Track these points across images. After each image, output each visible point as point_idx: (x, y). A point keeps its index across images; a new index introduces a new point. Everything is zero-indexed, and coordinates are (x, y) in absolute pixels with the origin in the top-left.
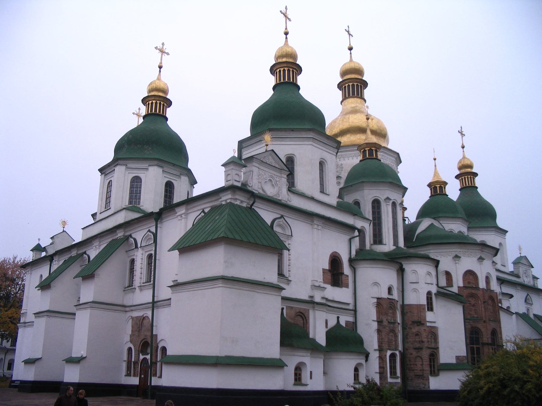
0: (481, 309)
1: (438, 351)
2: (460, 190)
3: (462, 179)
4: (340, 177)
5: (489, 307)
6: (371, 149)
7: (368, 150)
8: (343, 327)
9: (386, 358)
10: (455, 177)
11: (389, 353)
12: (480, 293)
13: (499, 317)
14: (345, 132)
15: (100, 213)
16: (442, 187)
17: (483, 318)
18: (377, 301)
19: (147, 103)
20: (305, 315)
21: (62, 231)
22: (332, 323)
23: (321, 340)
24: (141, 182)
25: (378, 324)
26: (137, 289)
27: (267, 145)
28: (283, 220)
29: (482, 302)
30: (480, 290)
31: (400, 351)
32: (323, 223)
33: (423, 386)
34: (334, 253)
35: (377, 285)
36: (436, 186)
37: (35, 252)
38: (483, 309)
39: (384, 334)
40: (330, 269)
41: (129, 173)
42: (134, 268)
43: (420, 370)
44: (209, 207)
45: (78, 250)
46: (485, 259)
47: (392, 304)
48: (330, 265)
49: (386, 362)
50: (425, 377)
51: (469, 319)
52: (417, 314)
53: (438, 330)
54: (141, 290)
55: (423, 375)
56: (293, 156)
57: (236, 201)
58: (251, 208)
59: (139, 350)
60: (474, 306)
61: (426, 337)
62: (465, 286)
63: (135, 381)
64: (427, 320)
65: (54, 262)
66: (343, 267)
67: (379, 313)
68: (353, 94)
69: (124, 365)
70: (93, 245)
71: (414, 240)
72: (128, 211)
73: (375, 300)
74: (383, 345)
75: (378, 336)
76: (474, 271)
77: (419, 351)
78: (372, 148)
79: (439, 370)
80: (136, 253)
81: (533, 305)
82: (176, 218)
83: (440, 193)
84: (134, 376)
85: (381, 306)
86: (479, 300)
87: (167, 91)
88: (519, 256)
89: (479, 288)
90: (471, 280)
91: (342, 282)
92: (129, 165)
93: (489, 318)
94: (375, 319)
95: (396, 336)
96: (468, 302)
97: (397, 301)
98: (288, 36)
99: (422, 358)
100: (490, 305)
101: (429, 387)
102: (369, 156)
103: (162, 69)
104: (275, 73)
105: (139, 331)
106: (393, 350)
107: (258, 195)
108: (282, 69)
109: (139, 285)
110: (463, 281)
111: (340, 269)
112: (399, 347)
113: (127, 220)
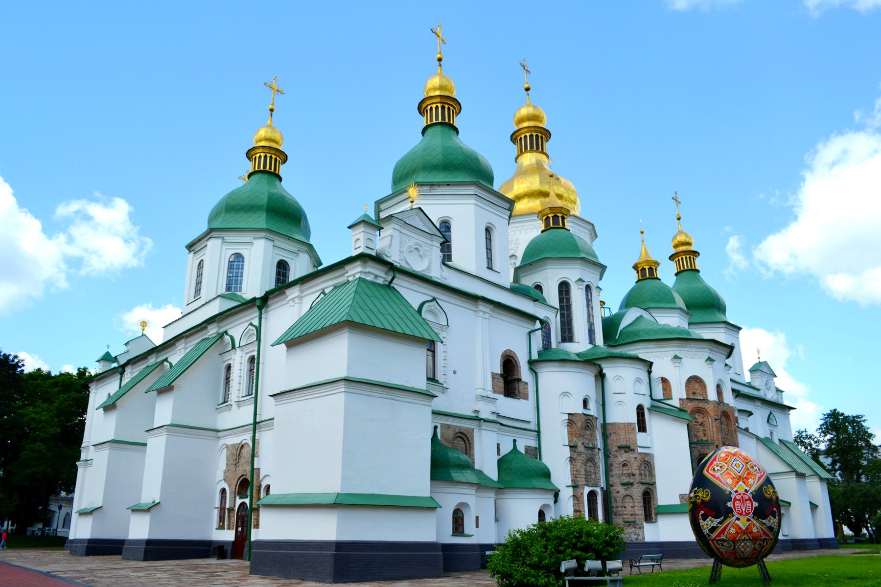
0: (713, 429)
1: (655, 487)
2: (676, 275)
3: (679, 260)
4: (514, 255)
5: (723, 427)
6: (556, 215)
7: (553, 217)
8: (522, 454)
9: (583, 498)
10: (668, 257)
11: (587, 490)
12: (710, 408)
13: (737, 440)
14: (521, 197)
15: (187, 305)
16: (653, 269)
17: (715, 442)
18: (569, 417)
19: (254, 157)
20: (468, 436)
21: (141, 335)
22: (506, 449)
23: (492, 472)
24: (243, 261)
25: (570, 450)
26: (234, 405)
27: (412, 202)
28: (435, 305)
29: (714, 420)
32: (491, 310)
33: (636, 536)
34: (507, 352)
35: (569, 397)
36: (645, 267)
37: (102, 364)
38: (714, 429)
39: (580, 464)
40: (502, 373)
41: (226, 249)
42: (230, 378)
43: (631, 515)
44: (332, 286)
45: (157, 357)
46: (714, 361)
47: (589, 421)
48: (502, 368)
49: (583, 503)
51: (696, 444)
52: (625, 437)
53: (653, 459)
54: (239, 407)
55: (635, 522)
56: (447, 220)
57: (368, 276)
58: (389, 286)
59: (235, 491)
60: (701, 424)
62: (689, 397)
63: (228, 536)
64: (639, 444)
65: (126, 375)
66: (520, 371)
67: (570, 434)
68: (532, 147)
69: (216, 514)
70: (177, 348)
71: (617, 337)
72: (222, 299)
73: (566, 417)
74: (578, 479)
75: (572, 466)
76: (700, 378)
77: (628, 488)
78: (557, 214)
79: (656, 514)
80: (233, 355)
81: (778, 427)
82: (286, 304)
83: (650, 277)
84: (229, 528)
85: (574, 425)
86: (709, 416)
87: (281, 142)
88: (758, 362)
90: (697, 389)
91: (519, 392)
92: (227, 239)
93: (723, 441)
94: (567, 444)
95: (595, 465)
96: (695, 420)
97: (597, 418)
98: (442, 63)
99: (633, 499)
102: (553, 225)
103: (273, 113)
104: (425, 111)
105: (236, 464)
106: (592, 486)
107: (401, 268)
108: (434, 106)
109: (237, 400)
110: (687, 391)
111: (516, 374)
112: (600, 482)
113: (221, 311)
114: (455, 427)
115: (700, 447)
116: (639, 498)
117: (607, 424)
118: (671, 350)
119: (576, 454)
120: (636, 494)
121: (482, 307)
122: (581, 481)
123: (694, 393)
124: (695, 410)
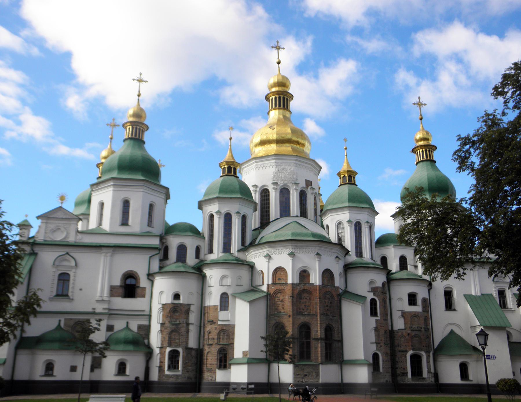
11: (168, 350)
18: (162, 306)
29: (289, 297)
30: (288, 285)
31: (188, 349)
43: (211, 364)
50: (213, 371)
61: (216, 334)
66: (139, 281)
73: (161, 306)
79: (230, 365)
89: (287, 283)
90: (282, 276)
100: (306, 299)
101: (215, 380)
106: (175, 347)
114: (75, 319)
115: (277, 317)
116: (215, 353)
117: (205, 307)
118: (265, 251)
119: (163, 328)
120: (214, 351)
121: (104, 250)
122: (166, 344)
123: (279, 279)
124: (277, 292)
